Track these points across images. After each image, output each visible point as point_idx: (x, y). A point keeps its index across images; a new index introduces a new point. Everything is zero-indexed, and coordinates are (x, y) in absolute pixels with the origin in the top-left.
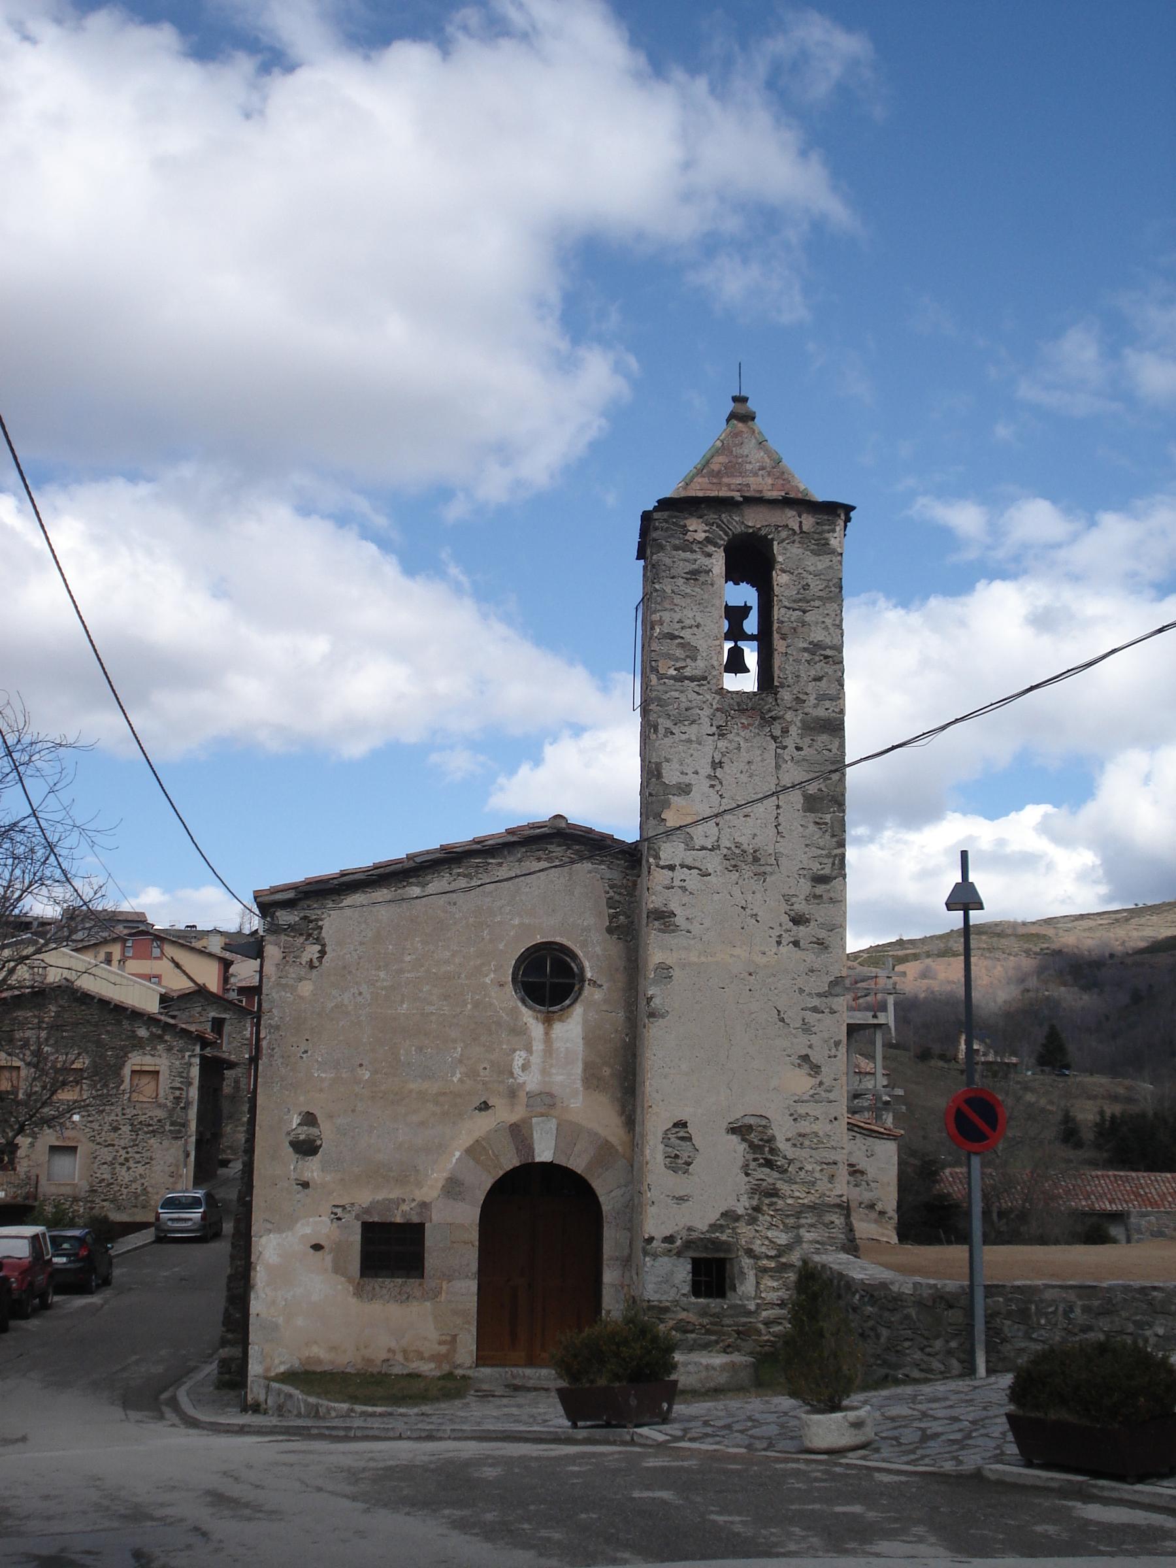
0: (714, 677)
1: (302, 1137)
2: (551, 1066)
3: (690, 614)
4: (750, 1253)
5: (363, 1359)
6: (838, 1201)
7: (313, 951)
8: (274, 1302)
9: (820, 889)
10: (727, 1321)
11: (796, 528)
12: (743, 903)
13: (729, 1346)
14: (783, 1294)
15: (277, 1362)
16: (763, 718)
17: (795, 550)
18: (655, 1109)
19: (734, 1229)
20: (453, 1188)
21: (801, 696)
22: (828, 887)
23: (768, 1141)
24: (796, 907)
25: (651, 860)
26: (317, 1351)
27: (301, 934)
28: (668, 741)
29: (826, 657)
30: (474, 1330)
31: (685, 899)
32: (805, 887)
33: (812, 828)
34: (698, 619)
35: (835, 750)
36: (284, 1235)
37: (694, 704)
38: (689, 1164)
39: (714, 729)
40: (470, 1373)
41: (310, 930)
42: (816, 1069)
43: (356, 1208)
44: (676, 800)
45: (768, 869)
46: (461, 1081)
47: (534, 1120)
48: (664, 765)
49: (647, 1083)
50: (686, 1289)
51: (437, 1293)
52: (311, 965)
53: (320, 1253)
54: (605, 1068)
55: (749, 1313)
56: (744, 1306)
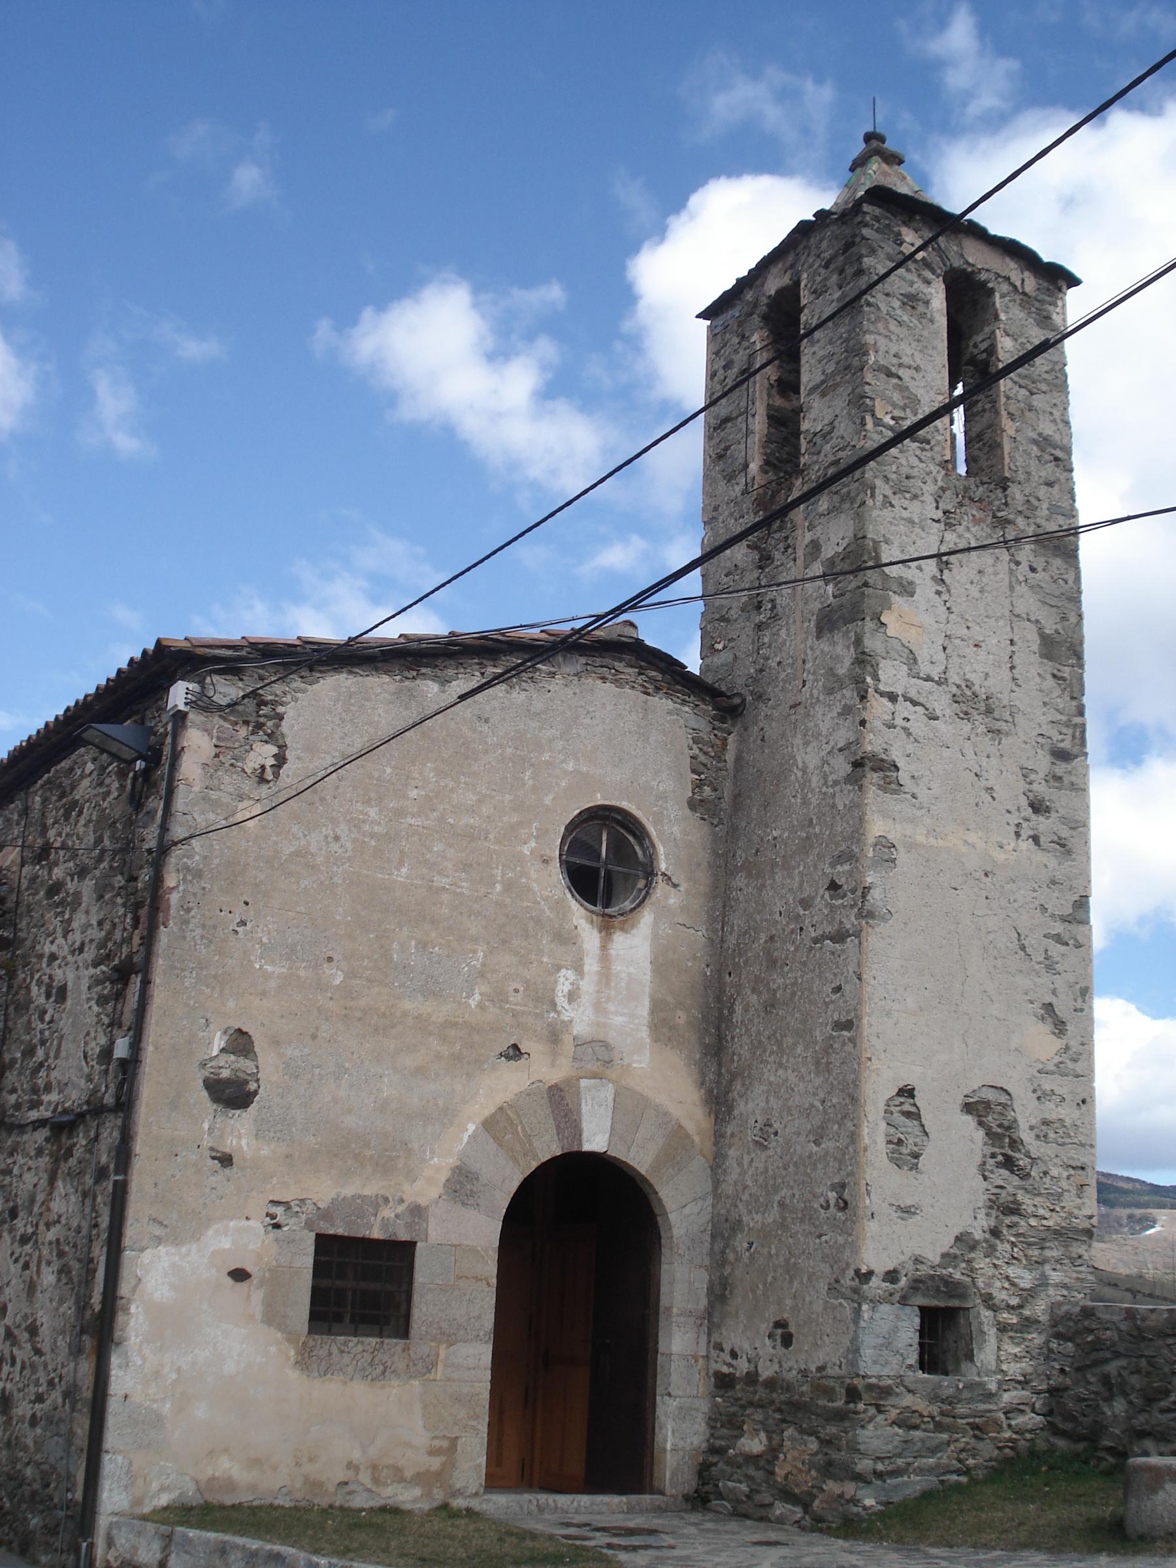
0: (938, 442)
1: (225, 1074)
2: (608, 999)
3: (908, 351)
4: (988, 1300)
5: (307, 1479)
6: (1086, 1224)
7: (264, 753)
8: (157, 1374)
9: (1061, 768)
10: (961, 1409)
11: (1018, 284)
12: (977, 769)
13: (962, 1450)
14: (1025, 1366)
15: (155, 1486)
16: (994, 516)
17: (1017, 313)
18: (875, 1064)
19: (969, 1261)
20: (462, 1185)
21: (1032, 500)
22: (1069, 767)
23: (1009, 1128)
24: (1035, 787)
25: (869, 679)
26: (227, 1467)
27: (246, 723)
28: (887, 513)
29: (1057, 459)
30: (484, 1429)
31: (910, 748)
32: (1043, 763)
33: (1050, 682)
34: (919, 362)
35: (1070, 582)
36: (184, 1250)
37: (914, 472)
38: (916, 1156)
39: (939, 514)
40: (475, 1504)
41: (260, 717)
42: (1060, 1027)
43: (309, 1207)
44: (896, 599)
45: (1004, 727)
46: (481, 1006)
47: (584, 1083)
48: (884, 546)
49: (865, 1021)
50: (913, 1358)
51: (431, 1366)
52: (262, 780)
53: (243, 1286)
54: (679, 1013)
55: (989, 1396)
56: (981, 1385)
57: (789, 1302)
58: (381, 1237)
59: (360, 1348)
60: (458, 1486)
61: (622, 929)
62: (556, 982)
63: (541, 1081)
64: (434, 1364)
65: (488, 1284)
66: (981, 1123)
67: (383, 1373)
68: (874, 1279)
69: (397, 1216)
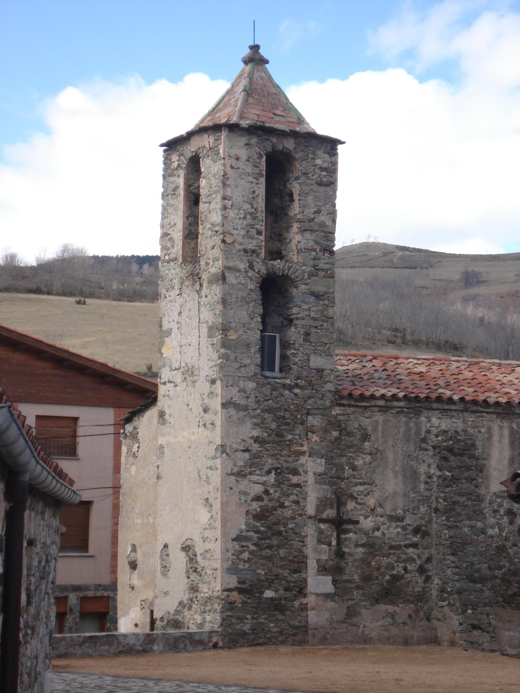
66: (187, 555)
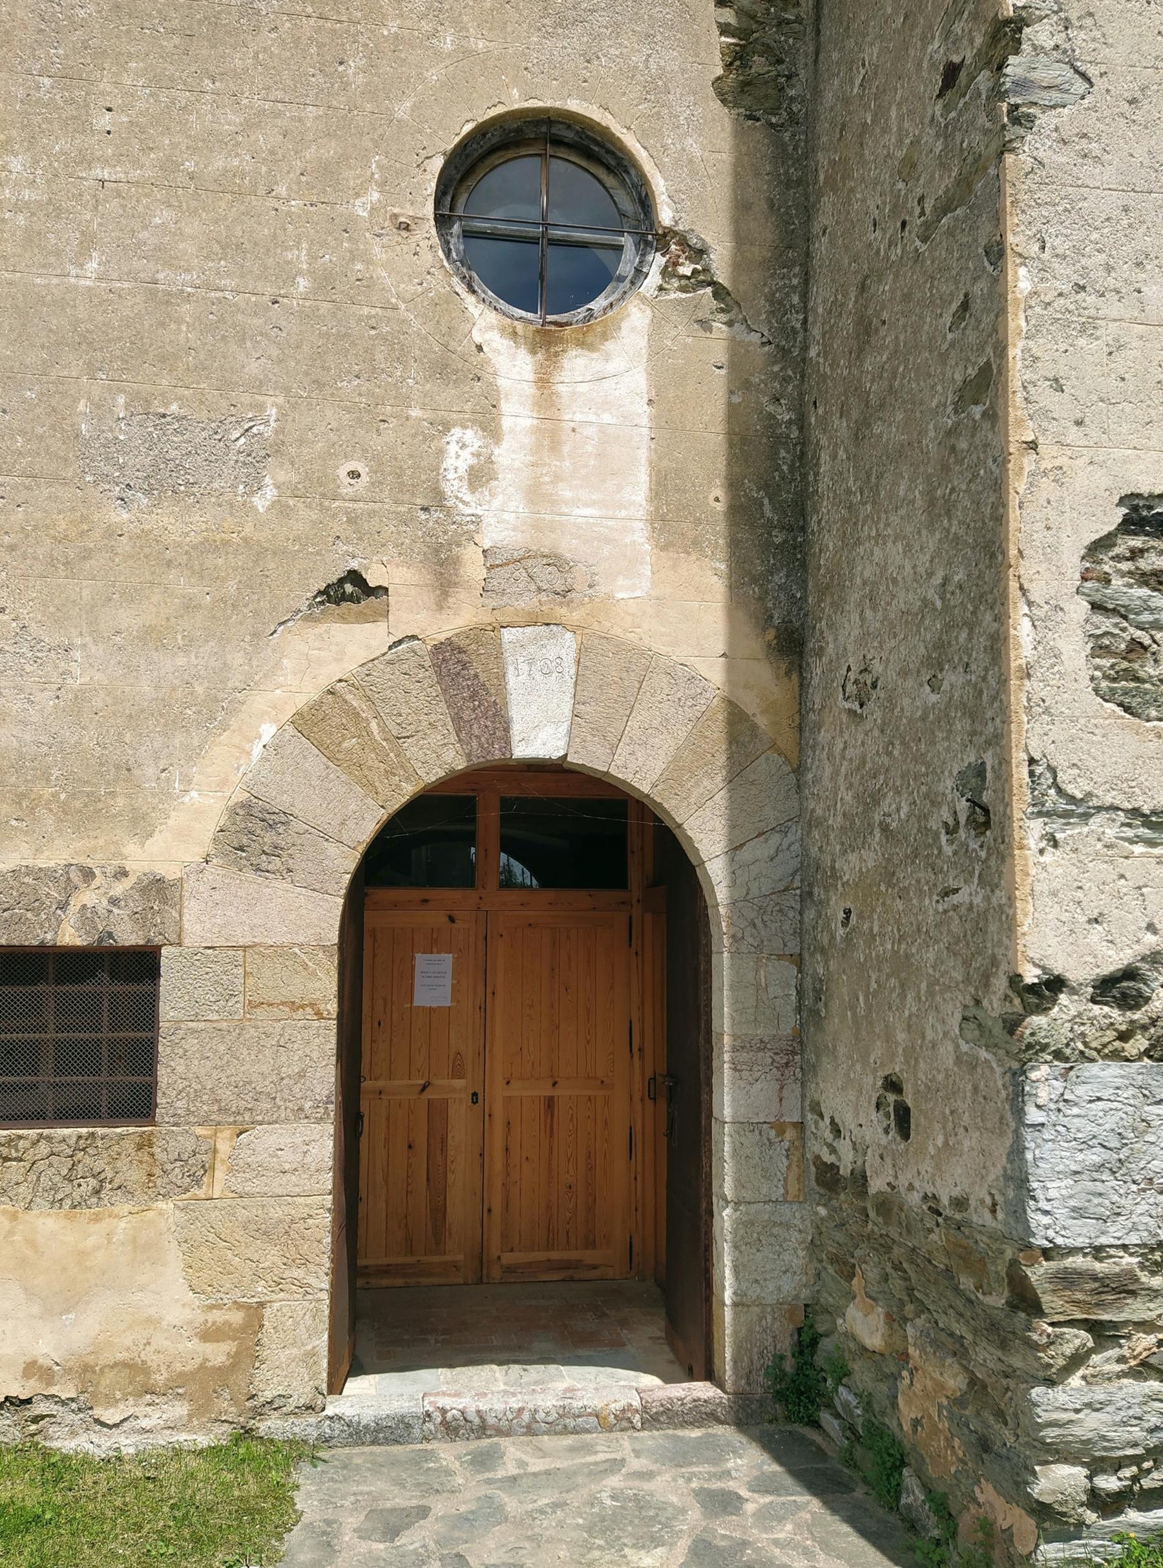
2: (557, 478)
20: (255, 836)
46: (281, 509)
51: (200, 1170)
57: (901, 1036)
58: (79, 942)
59: (44, 1148)
60: (268, 1395)
61: (581, 344)
62: (441, 453)
63: (414, 637)
64: (208, 1169)
65: (318, 1014)
67: (97, 1192)
68: (1063, 998)
69: (114, 901)
